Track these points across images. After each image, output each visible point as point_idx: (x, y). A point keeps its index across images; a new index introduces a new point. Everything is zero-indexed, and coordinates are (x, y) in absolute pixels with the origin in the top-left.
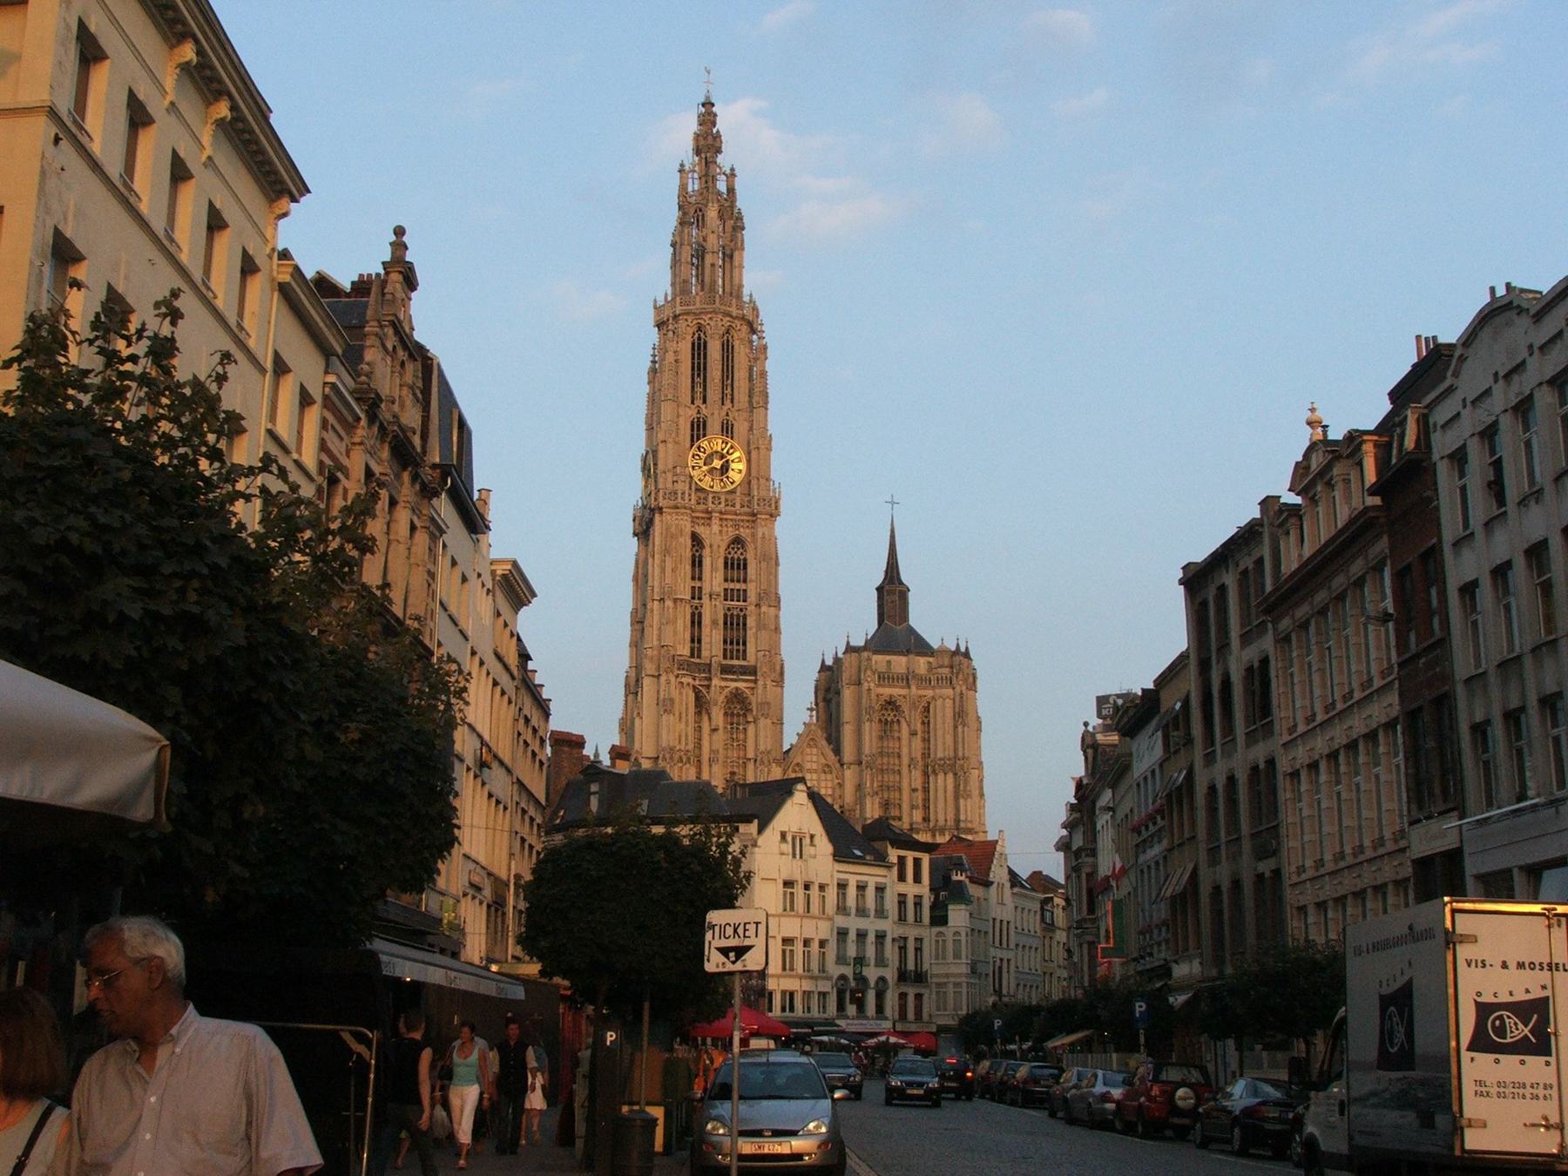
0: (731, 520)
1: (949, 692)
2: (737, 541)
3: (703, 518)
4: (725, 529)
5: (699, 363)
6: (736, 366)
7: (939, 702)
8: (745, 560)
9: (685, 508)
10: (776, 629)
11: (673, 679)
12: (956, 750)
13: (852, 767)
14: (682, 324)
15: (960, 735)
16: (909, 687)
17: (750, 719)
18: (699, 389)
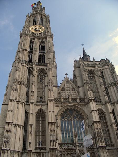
0: (41, 39)
1: (107, 67)
2: (42, 42)
3: (33, 38)
4: (39, 40)
5: (35, 21)
6: (43, 21)
7: (105, 70)
8: (45, 46)
9: (28, 34)
10: (53, 57)
11: (20, 64)
12: (114, 80)
13: (81, 87)
14: (31, 17)
15: (114, 76)
16: (95, 67)
17: (47, 76)
18: (34, 24)
